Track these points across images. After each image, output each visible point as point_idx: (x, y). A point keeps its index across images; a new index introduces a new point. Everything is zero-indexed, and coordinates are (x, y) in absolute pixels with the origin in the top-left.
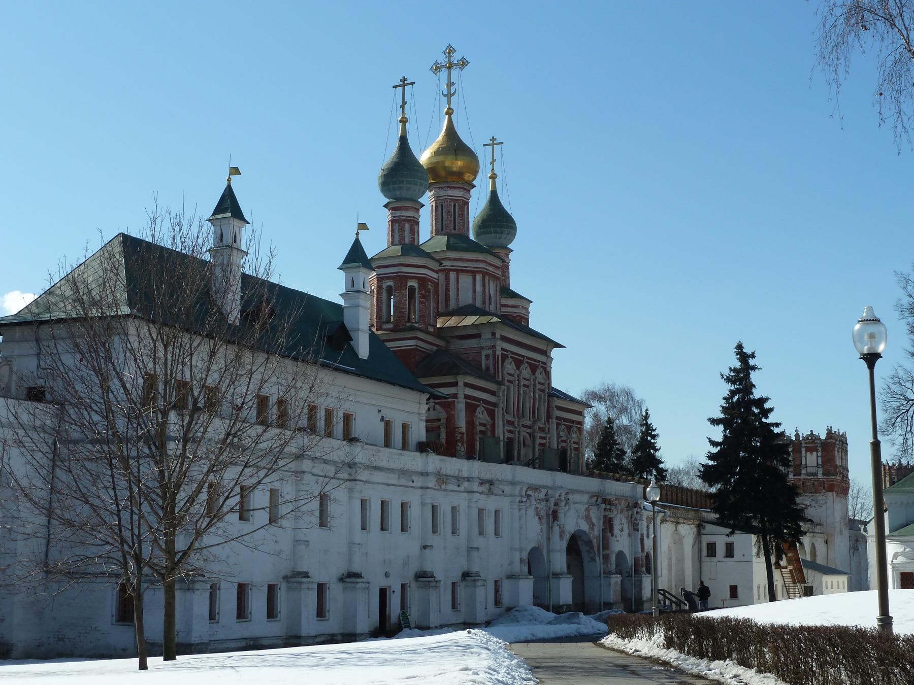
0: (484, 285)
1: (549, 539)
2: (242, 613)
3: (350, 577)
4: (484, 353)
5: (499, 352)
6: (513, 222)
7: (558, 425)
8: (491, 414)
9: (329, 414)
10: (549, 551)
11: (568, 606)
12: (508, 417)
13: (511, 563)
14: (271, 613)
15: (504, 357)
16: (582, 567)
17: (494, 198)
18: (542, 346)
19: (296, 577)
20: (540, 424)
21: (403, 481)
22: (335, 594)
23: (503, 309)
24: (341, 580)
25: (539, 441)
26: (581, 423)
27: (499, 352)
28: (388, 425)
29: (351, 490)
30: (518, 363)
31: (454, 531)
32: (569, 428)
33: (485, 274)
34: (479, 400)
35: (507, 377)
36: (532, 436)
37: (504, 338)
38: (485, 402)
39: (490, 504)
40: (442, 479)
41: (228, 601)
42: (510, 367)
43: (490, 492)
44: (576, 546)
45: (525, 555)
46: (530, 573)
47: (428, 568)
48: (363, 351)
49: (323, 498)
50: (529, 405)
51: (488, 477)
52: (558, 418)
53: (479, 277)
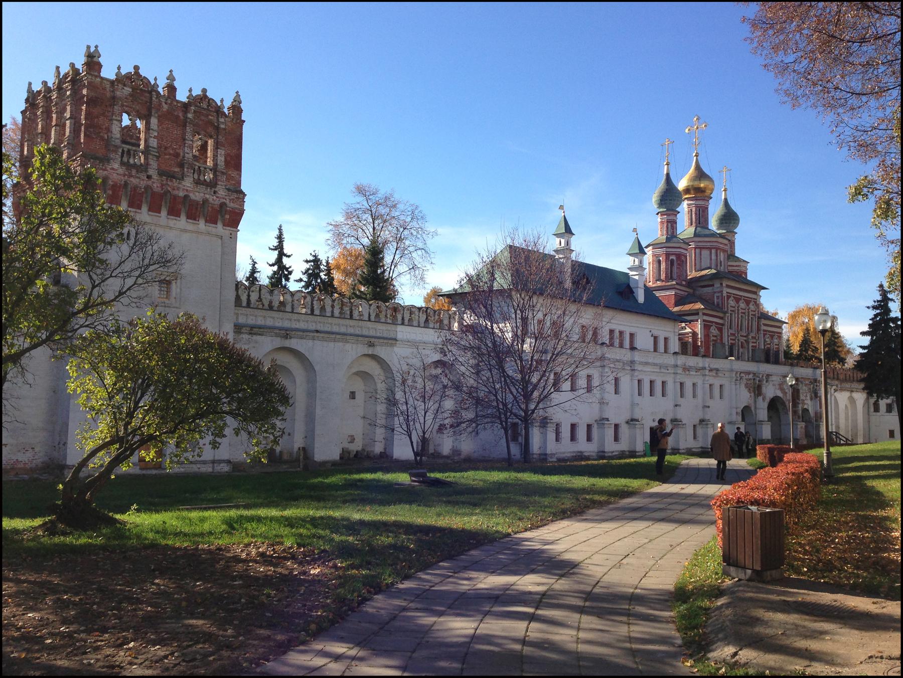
0: (717, 256)
1: (755, 402)
2: (573, 438)
3: (632, 421)
4: (716, 295)
5: (725, 294)
6: (737, 216)
7: (764, 335)
8: (720, 330)
9: (621, 333)
10: (755, 408)
11: (768, 440)
12: (730, 331)
13: (731, 414)
14: (589, 439)
15: (728, 297)
16: (779, 418)
17: (726, 203)
18: (754, 290)
19: (602, 421)
20: (753, 335)
21: (663, 370)
22: (624, 430)
23: (730, 268)
24: (627, 422)
25: (751, 344)
26: (781, 333)
27: (725, 294)
28: (656, 339)
29: (632, 376)
30: (737, 300)
31: (694, 396)
32: (772, 337)
33: (717, 249)
34: (712, 322)
35: (730, 309)
36: (747, 342)
37: (728, 286)
38: (716, 323)
39: (717, 383)
40: (686, 369)
41: (566, 432)
42: (732, 302)
43: (717, 376)
44: (775, 405)
45: (740, 410)
46: (743, 420)
47: (678, 417)
48: (641, 299)
49: (616, 380)
50: (745, 323)
51: (715, 366)
52: (764, 331)
53: (713, 251)
